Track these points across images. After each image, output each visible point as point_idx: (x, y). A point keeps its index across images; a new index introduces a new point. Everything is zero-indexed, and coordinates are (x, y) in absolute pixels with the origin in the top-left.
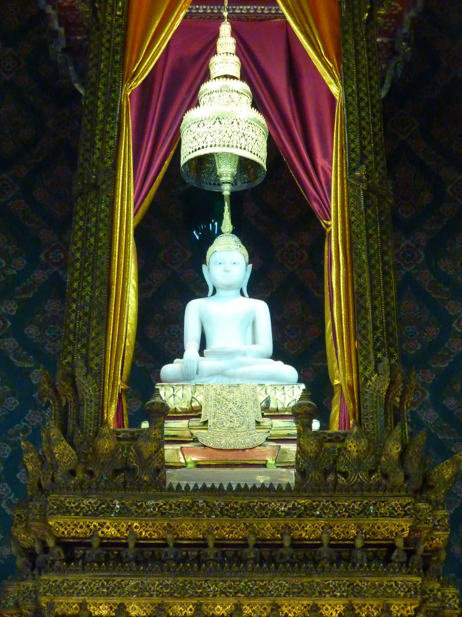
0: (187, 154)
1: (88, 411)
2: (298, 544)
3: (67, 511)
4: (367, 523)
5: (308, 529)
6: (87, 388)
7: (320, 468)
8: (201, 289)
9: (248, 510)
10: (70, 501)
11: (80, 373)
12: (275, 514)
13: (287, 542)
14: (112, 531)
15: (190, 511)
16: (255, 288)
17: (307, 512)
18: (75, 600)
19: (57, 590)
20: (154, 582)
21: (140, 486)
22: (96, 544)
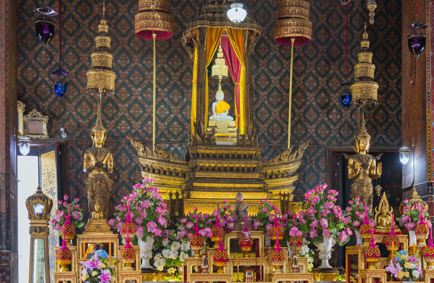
0: (213, 75)
1: (202, 130)
2: (237, 155)
3: (201, 149)
4: (249, 152)
5: (239, 152)
6: (202, 127)
7: (241, 142)
8: (215, 100)
9: (230, 149)
10: (201, 147)
11: (201, 123)
12: (234, 150)
13: (236, 155)
14: (208, 152)
15: (220, 149)
16: (224, 100)
17: (239, 150)
18: (203, 164)
19: (200, 162)
20: (215, 161)
21: (212, 145)
22: (205, 154)
